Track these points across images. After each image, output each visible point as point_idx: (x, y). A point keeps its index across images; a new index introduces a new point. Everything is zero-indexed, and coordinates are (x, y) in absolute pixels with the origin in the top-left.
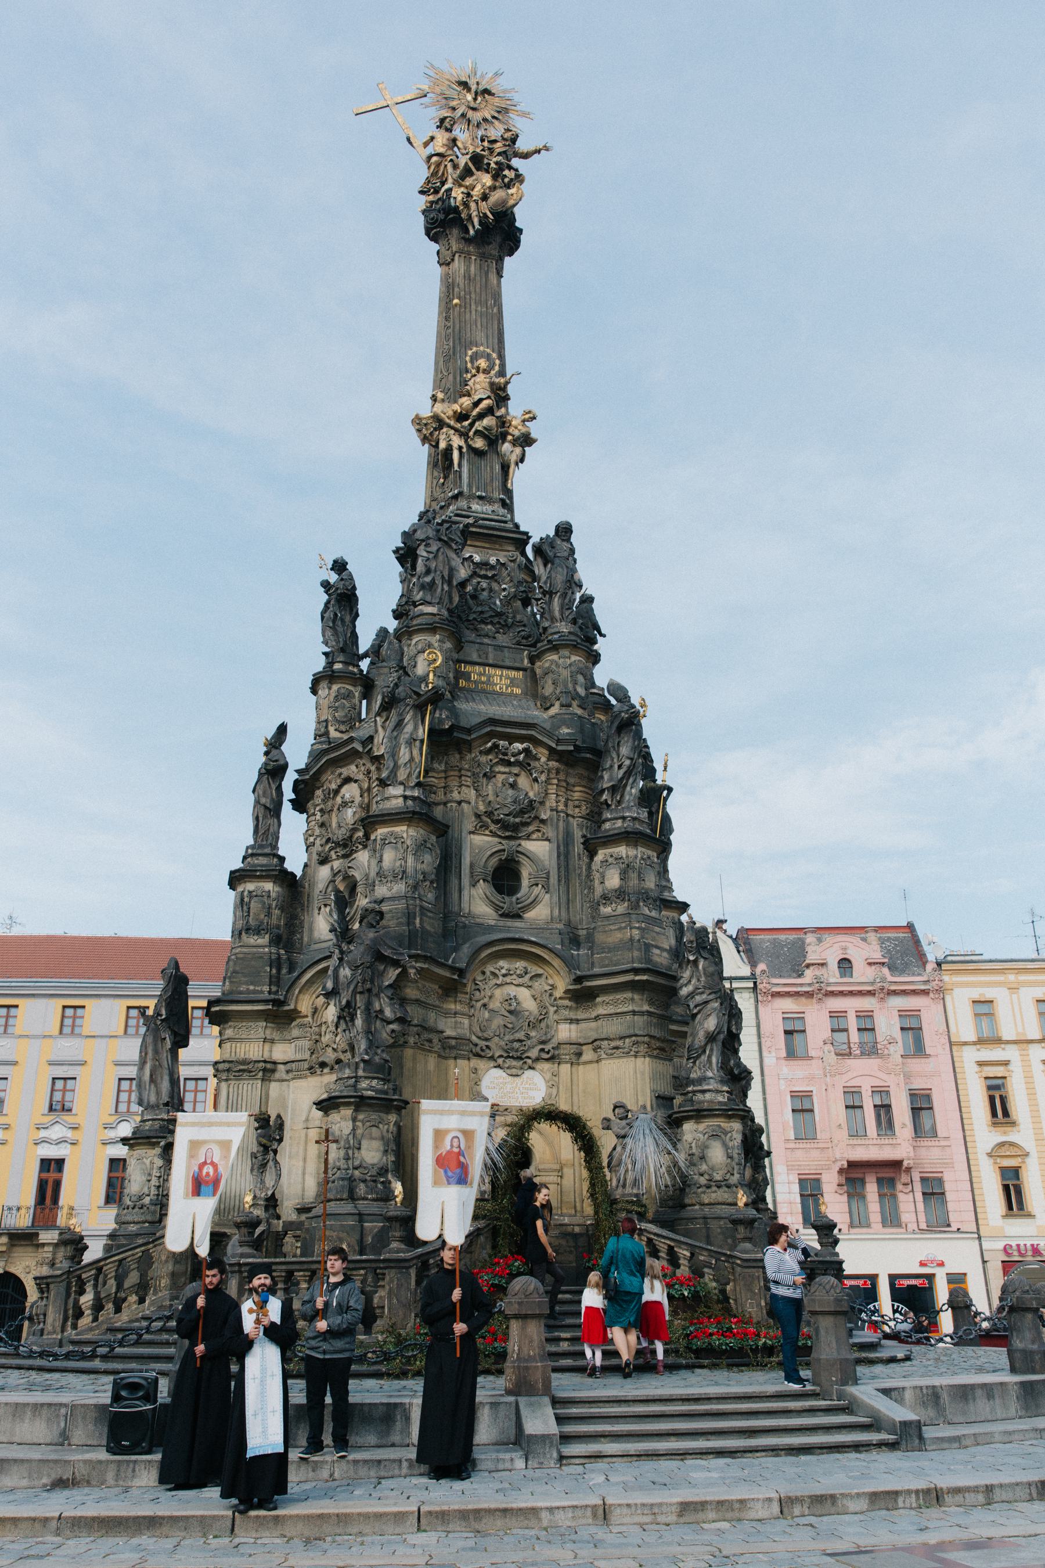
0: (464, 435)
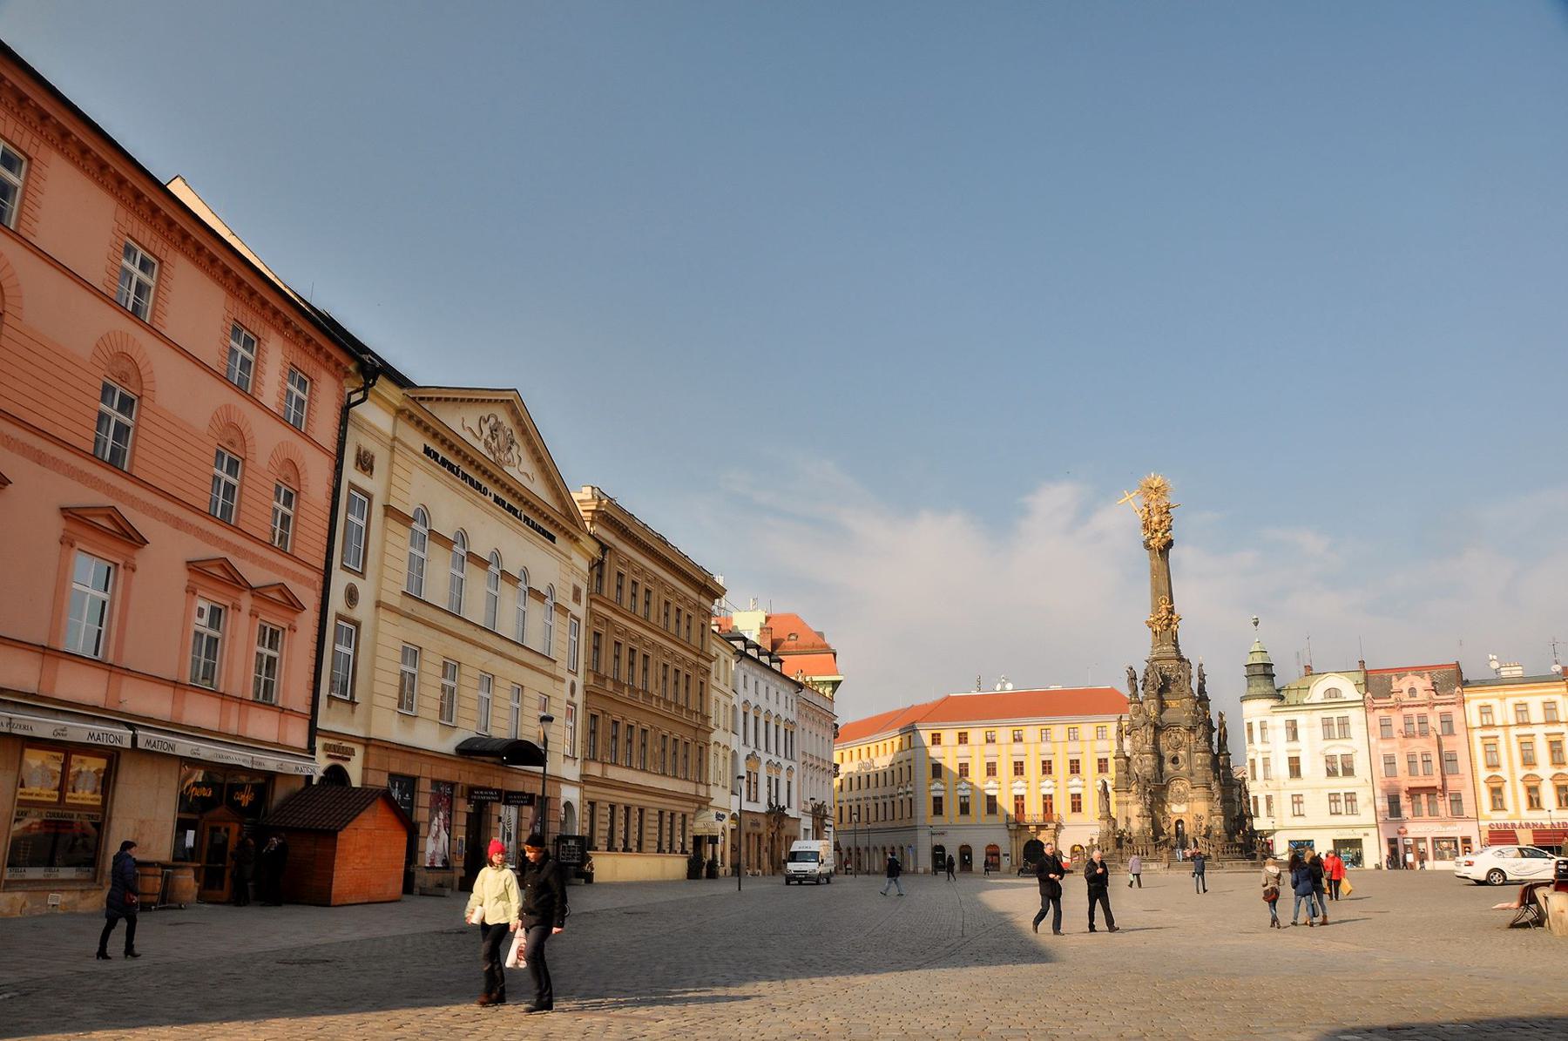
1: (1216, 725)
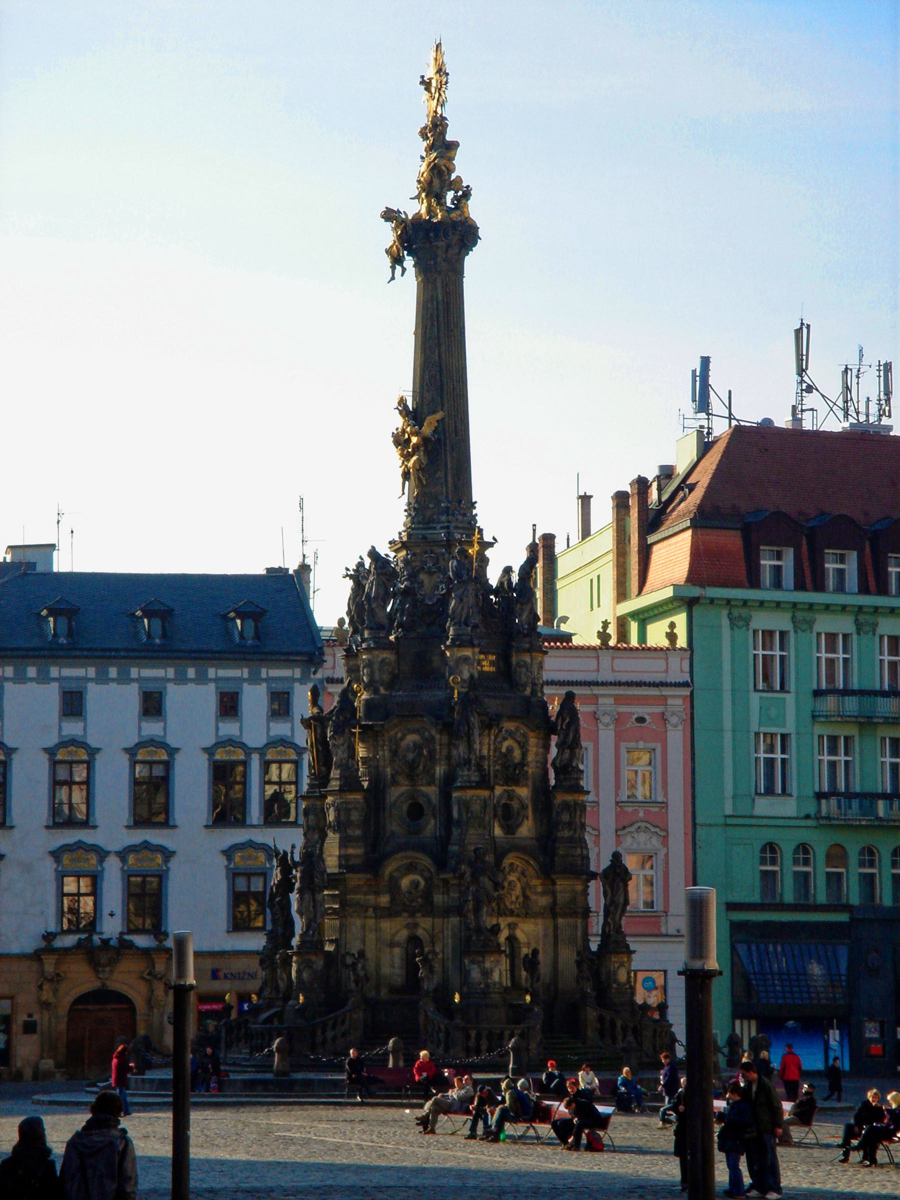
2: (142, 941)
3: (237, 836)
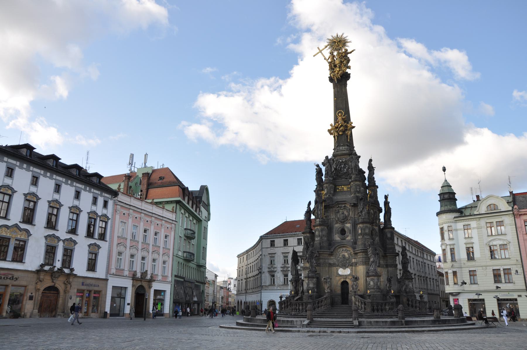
0: (337, 132)
1: (382, 205)
2: (66, 271)
3: (92, 241)
